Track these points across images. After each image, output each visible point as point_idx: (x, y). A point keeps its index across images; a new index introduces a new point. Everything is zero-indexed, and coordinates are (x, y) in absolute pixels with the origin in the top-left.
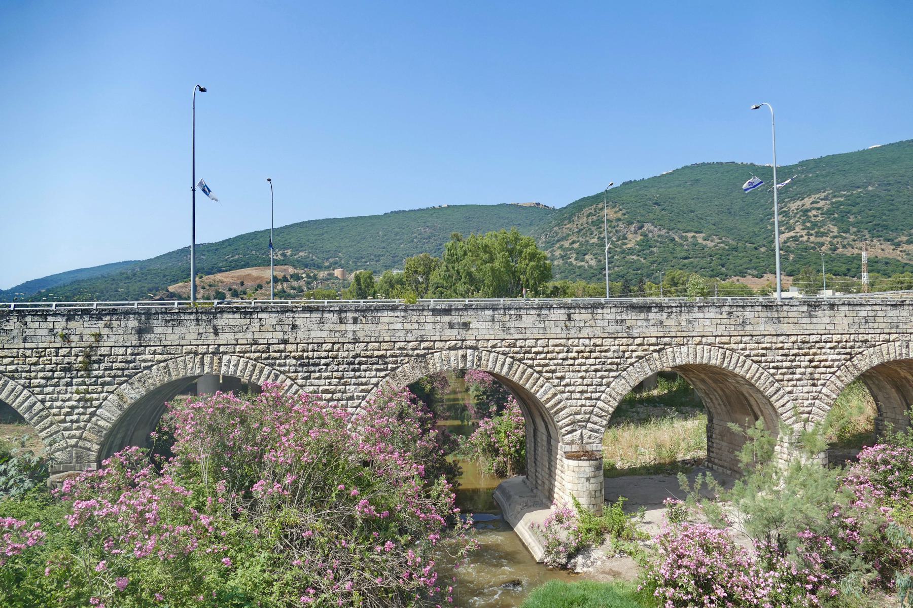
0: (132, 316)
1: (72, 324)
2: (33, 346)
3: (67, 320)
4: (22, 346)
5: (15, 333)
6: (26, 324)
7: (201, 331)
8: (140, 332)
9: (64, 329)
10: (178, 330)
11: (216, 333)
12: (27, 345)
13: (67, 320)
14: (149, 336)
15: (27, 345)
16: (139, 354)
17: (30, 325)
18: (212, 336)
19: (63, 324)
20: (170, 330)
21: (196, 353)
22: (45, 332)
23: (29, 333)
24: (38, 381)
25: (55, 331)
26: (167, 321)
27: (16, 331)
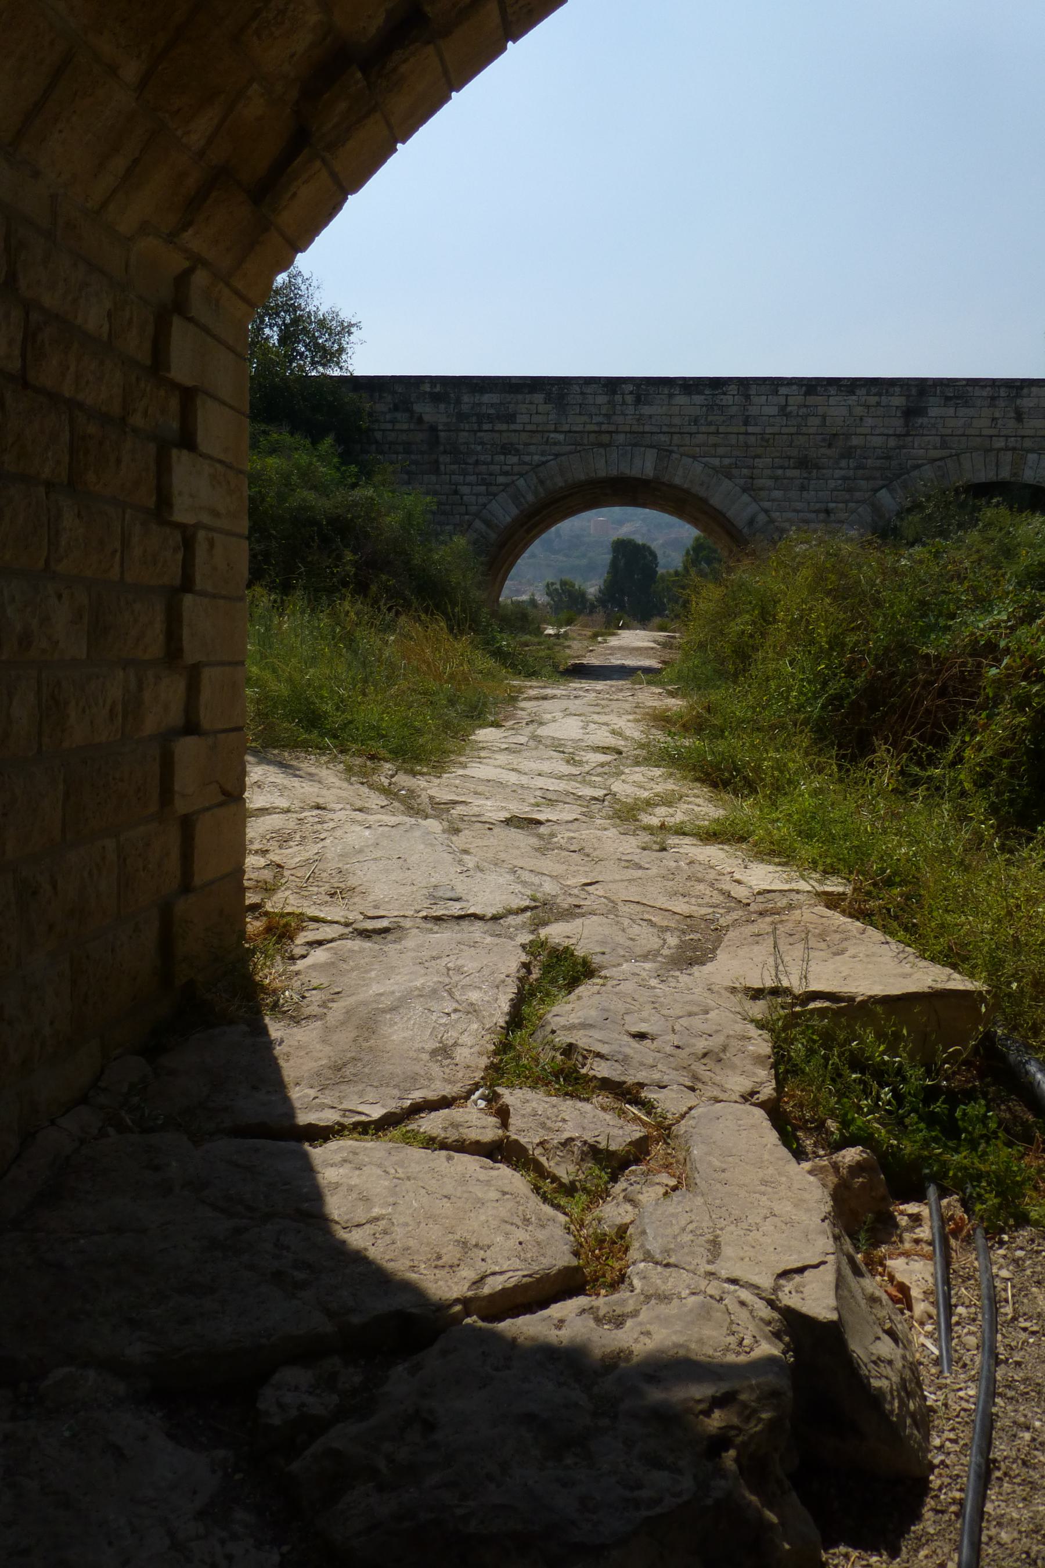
0: (897, 389)
1: (811, 400)
2: (757, 430)
3: (806, 394)
4: (742, 429)
5: (733, 410)
6: (748, 397)
7: (997, 415)
8: (911, 413)
9: (799, 406)
10: (962, 411)
11: (1019, 417)
12: (750, 429)
13: (806, 394)
14: (920, 421)
15: (750, 429)
16: (904, 447)
17: (755, 399)
18: (1012, 423)
19: (800, 399)
20: (951, 411)
21: (988, 450)
22: (773, 410)
23: (753, 411)
24: (763, 481)
25: (789, 409)
26: (948, 399)
27: (735, 408)
